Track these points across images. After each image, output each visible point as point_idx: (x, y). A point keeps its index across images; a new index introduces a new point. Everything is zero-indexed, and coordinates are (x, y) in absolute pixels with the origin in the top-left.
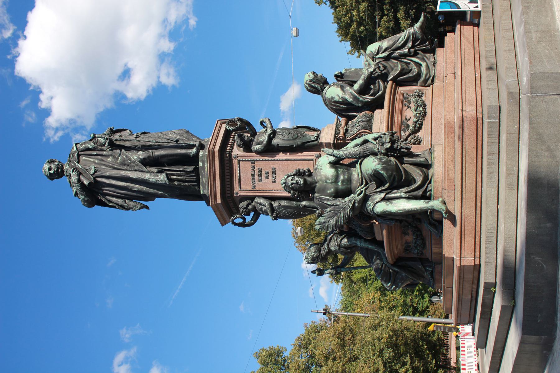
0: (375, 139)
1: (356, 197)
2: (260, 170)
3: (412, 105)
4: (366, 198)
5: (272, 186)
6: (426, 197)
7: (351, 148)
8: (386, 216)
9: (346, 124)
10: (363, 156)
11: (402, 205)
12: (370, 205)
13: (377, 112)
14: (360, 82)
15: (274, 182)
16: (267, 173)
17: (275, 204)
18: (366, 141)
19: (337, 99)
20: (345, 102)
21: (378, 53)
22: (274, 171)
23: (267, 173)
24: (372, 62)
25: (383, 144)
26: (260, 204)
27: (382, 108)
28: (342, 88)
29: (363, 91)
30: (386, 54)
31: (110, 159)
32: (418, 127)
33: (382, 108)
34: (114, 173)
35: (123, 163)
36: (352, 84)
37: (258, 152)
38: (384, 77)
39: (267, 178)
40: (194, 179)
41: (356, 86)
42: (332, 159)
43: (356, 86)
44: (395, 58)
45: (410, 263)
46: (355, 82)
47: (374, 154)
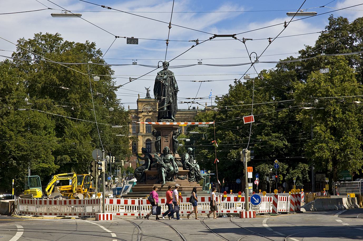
0: (177, 169)
1: (164, 165)
2: (168, 138)
3: (184, 176)
4: (164, 167)
5: (164, 142)
6: (166, 180)
7: (175, 163)
8: (162, 172)
9: (180, 160)
10: (173, 166)
11: (164, 175)
12: (164, 169)
13: (182, 168)
14: (190, 164)
15: (165, 142)
16: (167, 140)
17: (159, 142)
18: (176, 167)
19: (185, 157)
20: (185, 159)
21: (196, 168)
22: (168, 141)
23: (167, 140)
24: (194, 166)
25: (176, 171)
26: (159, 138)
27: (183, 169)
28: (188, 159)
29: (187, 164)
30: (196, 169)
31: (170, 89)
32: (178, 178)
33: (183, 169)
34: (166, 92)
35: (169, 95)
36: (189, 161)
37: (173, 137)
38: (191, 170)
39: (166, 139)
40: (165, 116)
41: (188, 163)
42: (172, 158)
43: (188, 163)
44: (195, 172)
45: (144, 177)
46: (189, 162)
47: (174, 169)
